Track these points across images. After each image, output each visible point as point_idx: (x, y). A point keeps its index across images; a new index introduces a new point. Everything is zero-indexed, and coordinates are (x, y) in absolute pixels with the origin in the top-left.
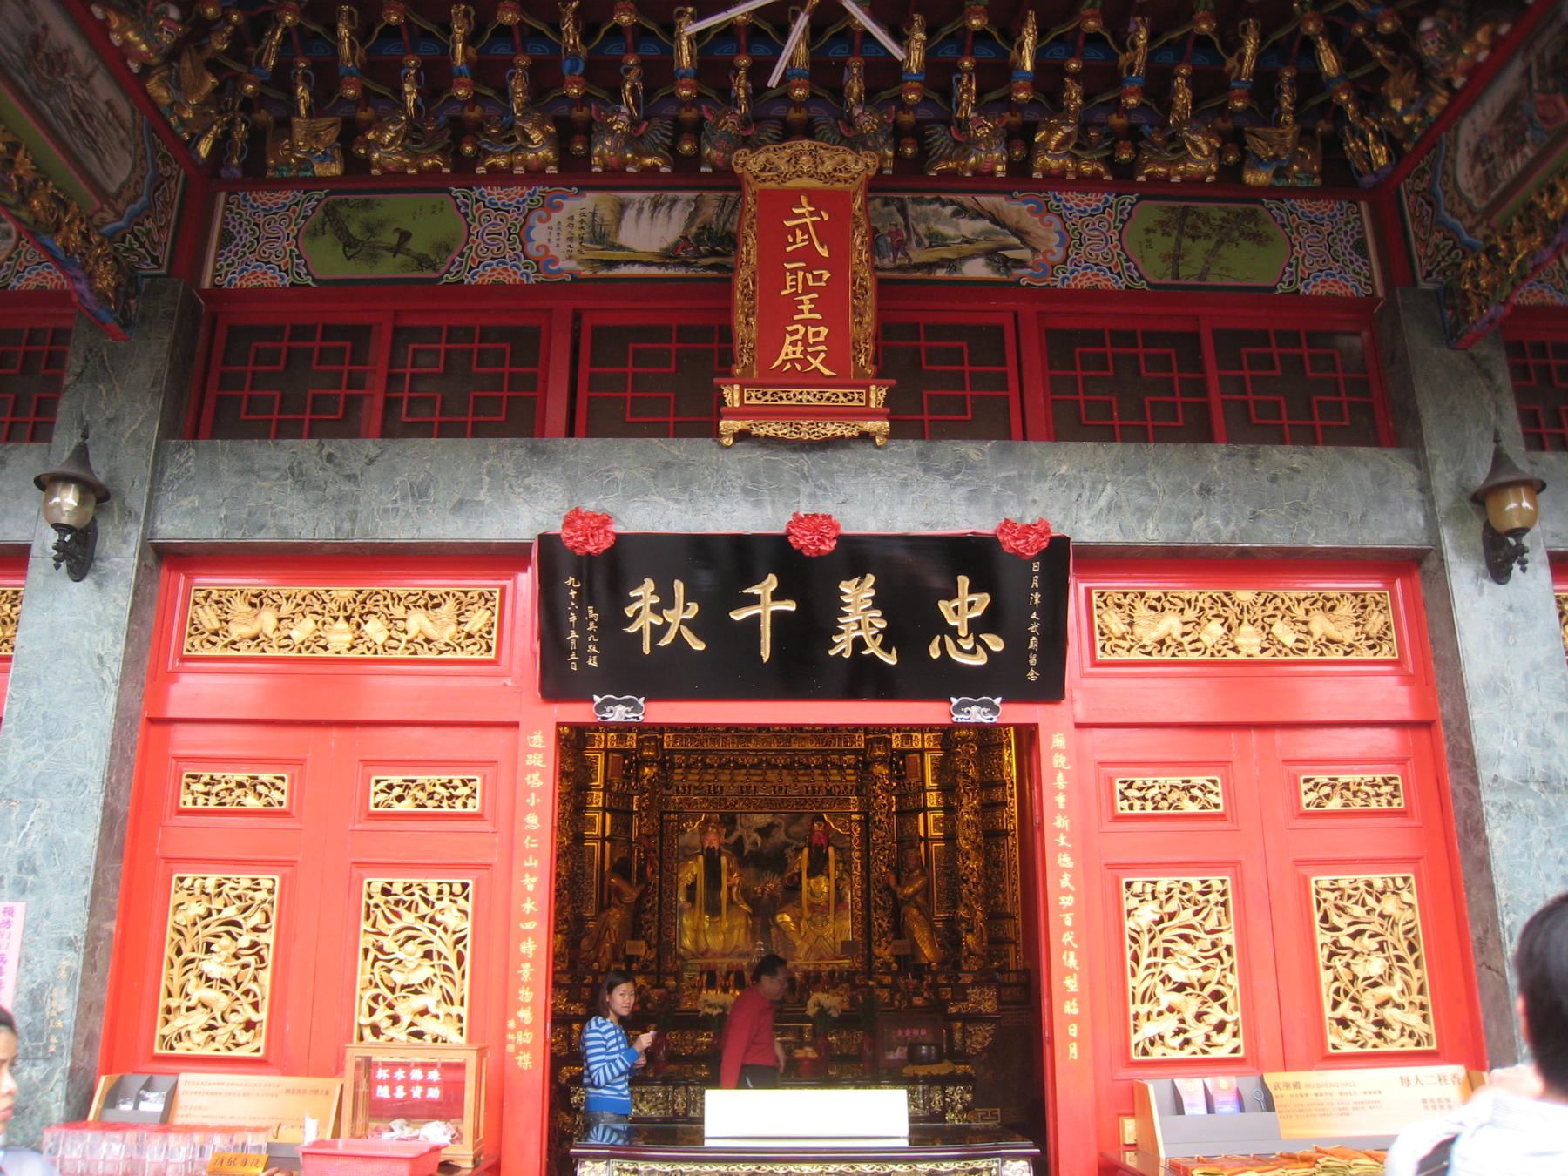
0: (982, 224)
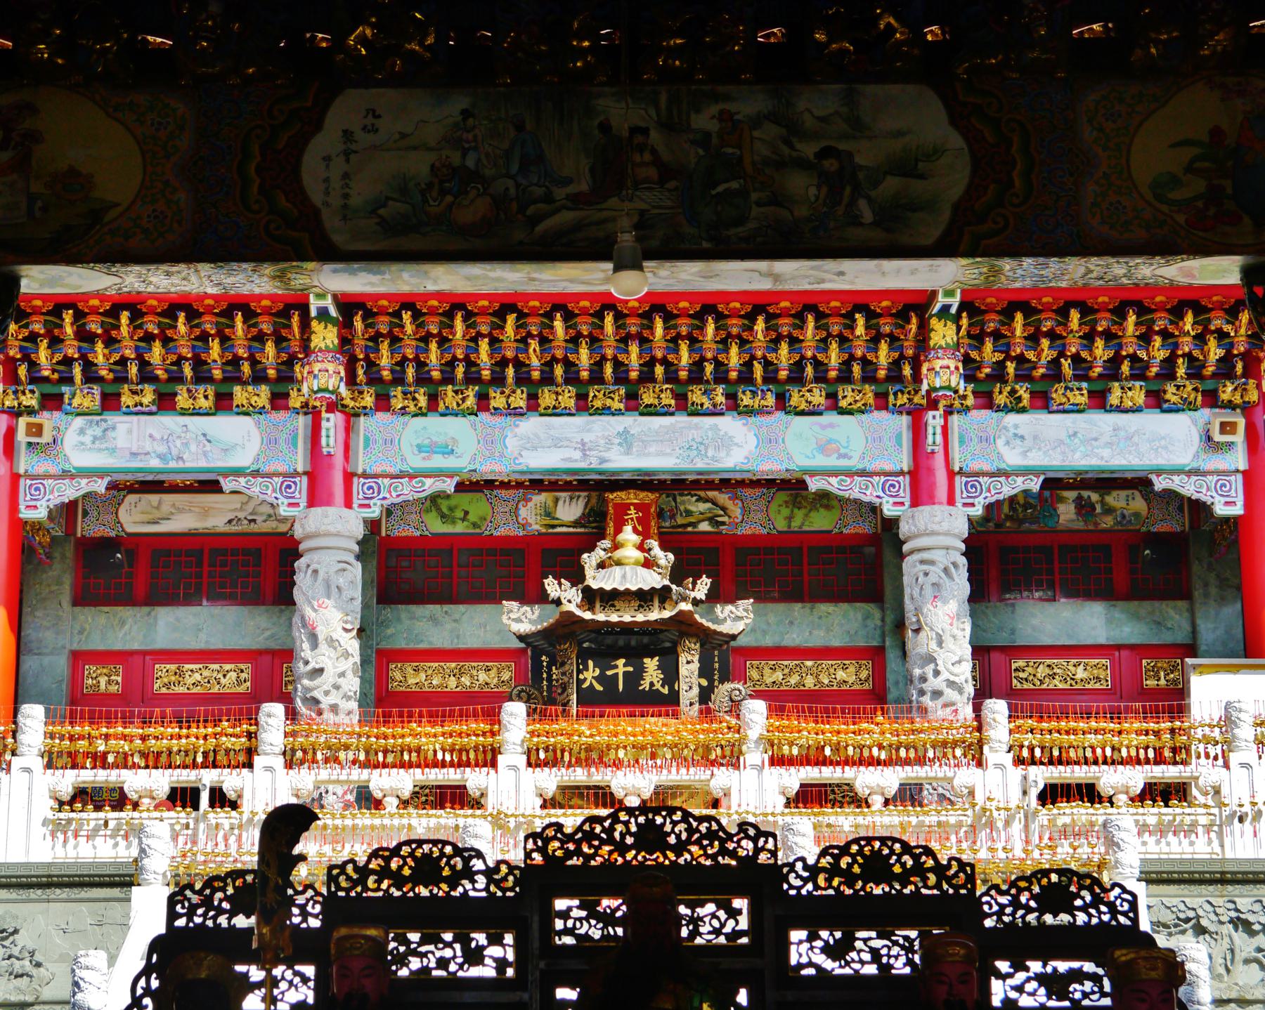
0: (709, 505)
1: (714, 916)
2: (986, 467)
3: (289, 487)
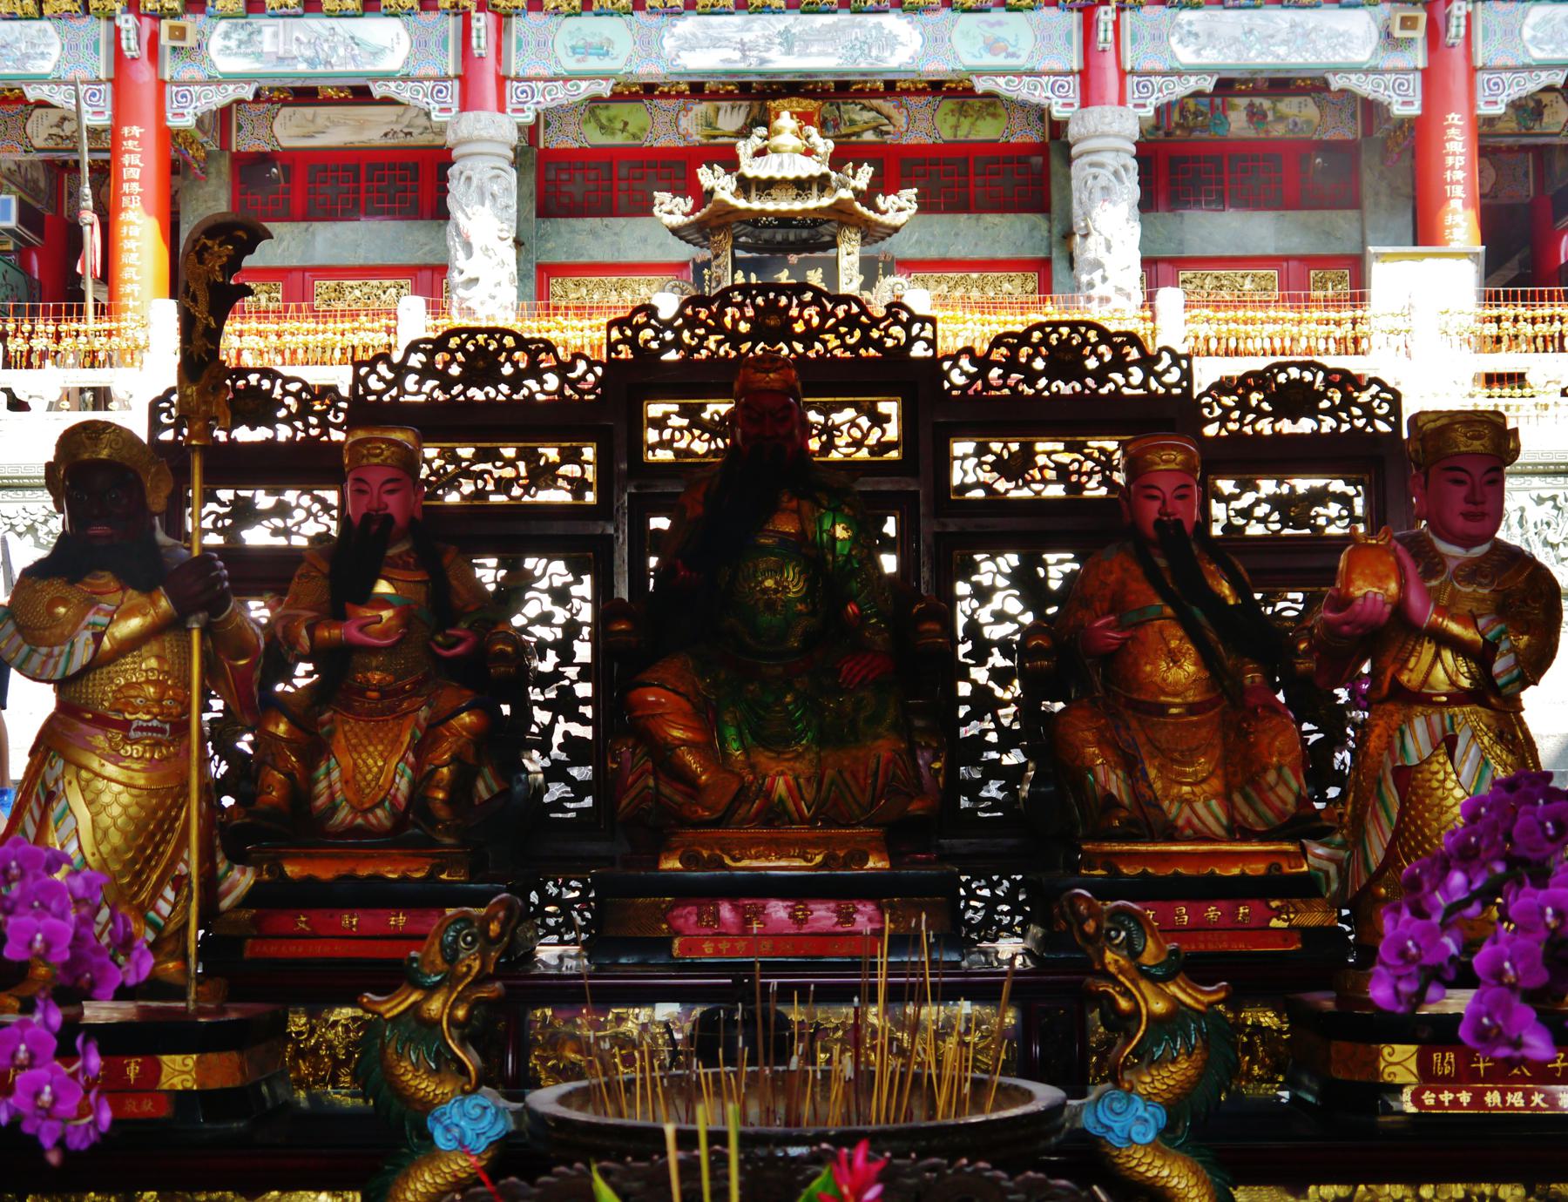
0: (873, 114)
1: (853, 424)
2: (1159, 66)
3: (440, 91)
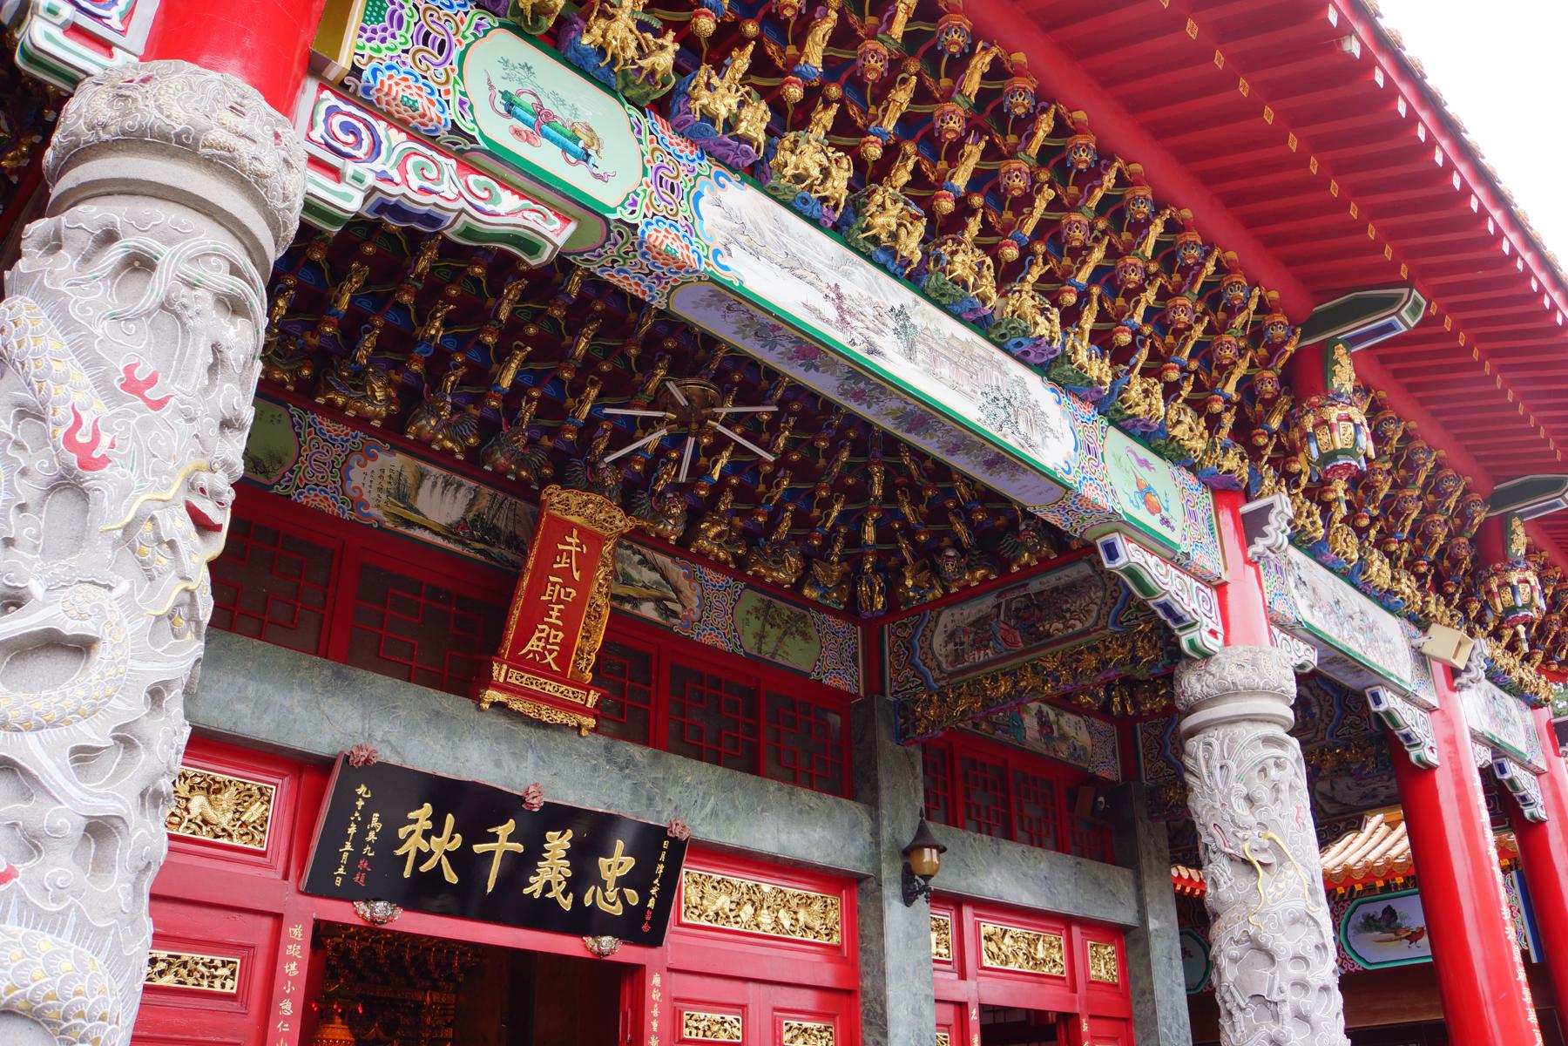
0: (655, 576)
